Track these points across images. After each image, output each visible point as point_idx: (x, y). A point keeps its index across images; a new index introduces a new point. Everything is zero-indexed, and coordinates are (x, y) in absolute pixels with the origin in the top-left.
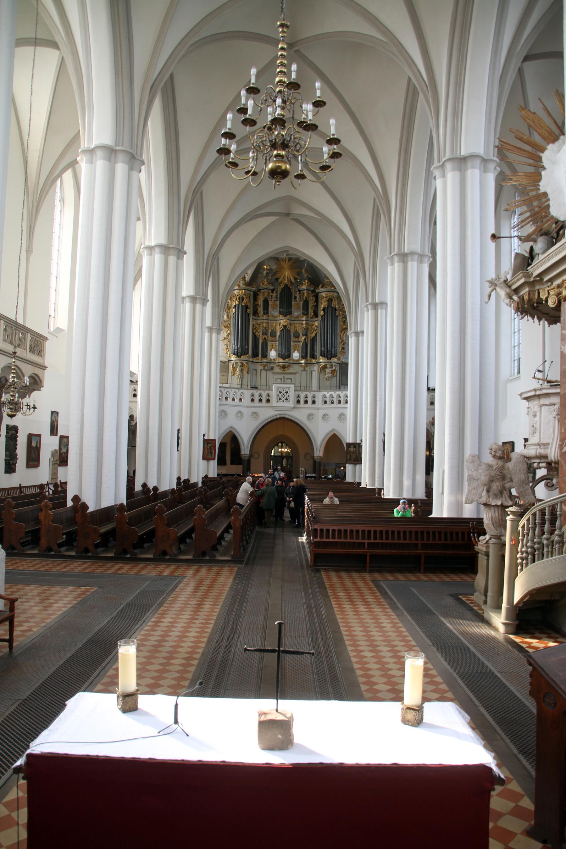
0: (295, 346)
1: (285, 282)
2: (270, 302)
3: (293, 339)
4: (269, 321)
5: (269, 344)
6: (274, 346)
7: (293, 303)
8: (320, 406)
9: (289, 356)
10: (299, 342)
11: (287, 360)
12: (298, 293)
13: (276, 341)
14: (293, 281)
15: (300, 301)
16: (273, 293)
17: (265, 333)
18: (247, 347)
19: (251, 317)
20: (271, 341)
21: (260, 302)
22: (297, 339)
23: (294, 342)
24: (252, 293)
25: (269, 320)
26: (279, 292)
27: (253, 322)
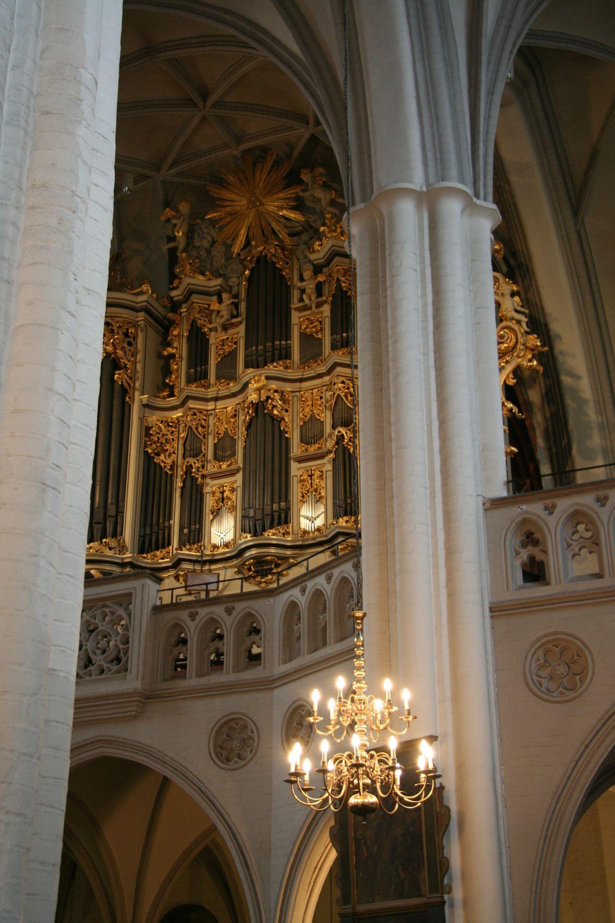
0: (305, 477)
1: (259, 249)
2: (213, 339)
3: (296, 448)
4: (211, 406)
5: (211, 486)
6: (225, 495)
7: (295, 317)
8: (281, 669)
9: (283, 518)
10: (322, 457)
11: (271, 535)
12: (307, 274)
13: (232, 473)
14: (283, 235)
15: (319, 305)
16: (220, 301)
17: (193, 449)
18: (112, 510)
19: (139, 399)
20: (215, 476)
21: (180, 348)
22: (312, 449)
23: (300, 460)
24: (141, 315)
25: (207, 400)
26: (243, 295)
27: (142, 419)
